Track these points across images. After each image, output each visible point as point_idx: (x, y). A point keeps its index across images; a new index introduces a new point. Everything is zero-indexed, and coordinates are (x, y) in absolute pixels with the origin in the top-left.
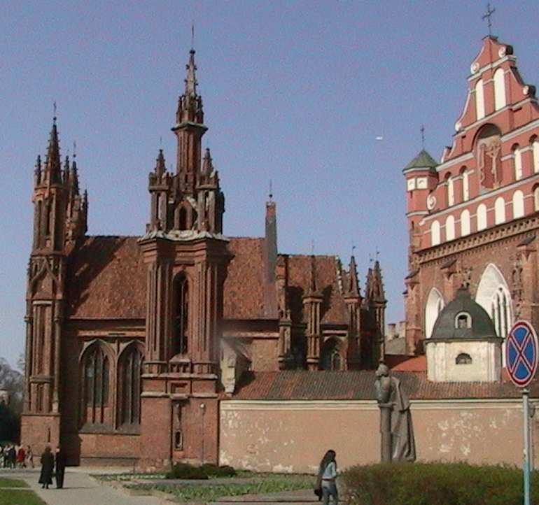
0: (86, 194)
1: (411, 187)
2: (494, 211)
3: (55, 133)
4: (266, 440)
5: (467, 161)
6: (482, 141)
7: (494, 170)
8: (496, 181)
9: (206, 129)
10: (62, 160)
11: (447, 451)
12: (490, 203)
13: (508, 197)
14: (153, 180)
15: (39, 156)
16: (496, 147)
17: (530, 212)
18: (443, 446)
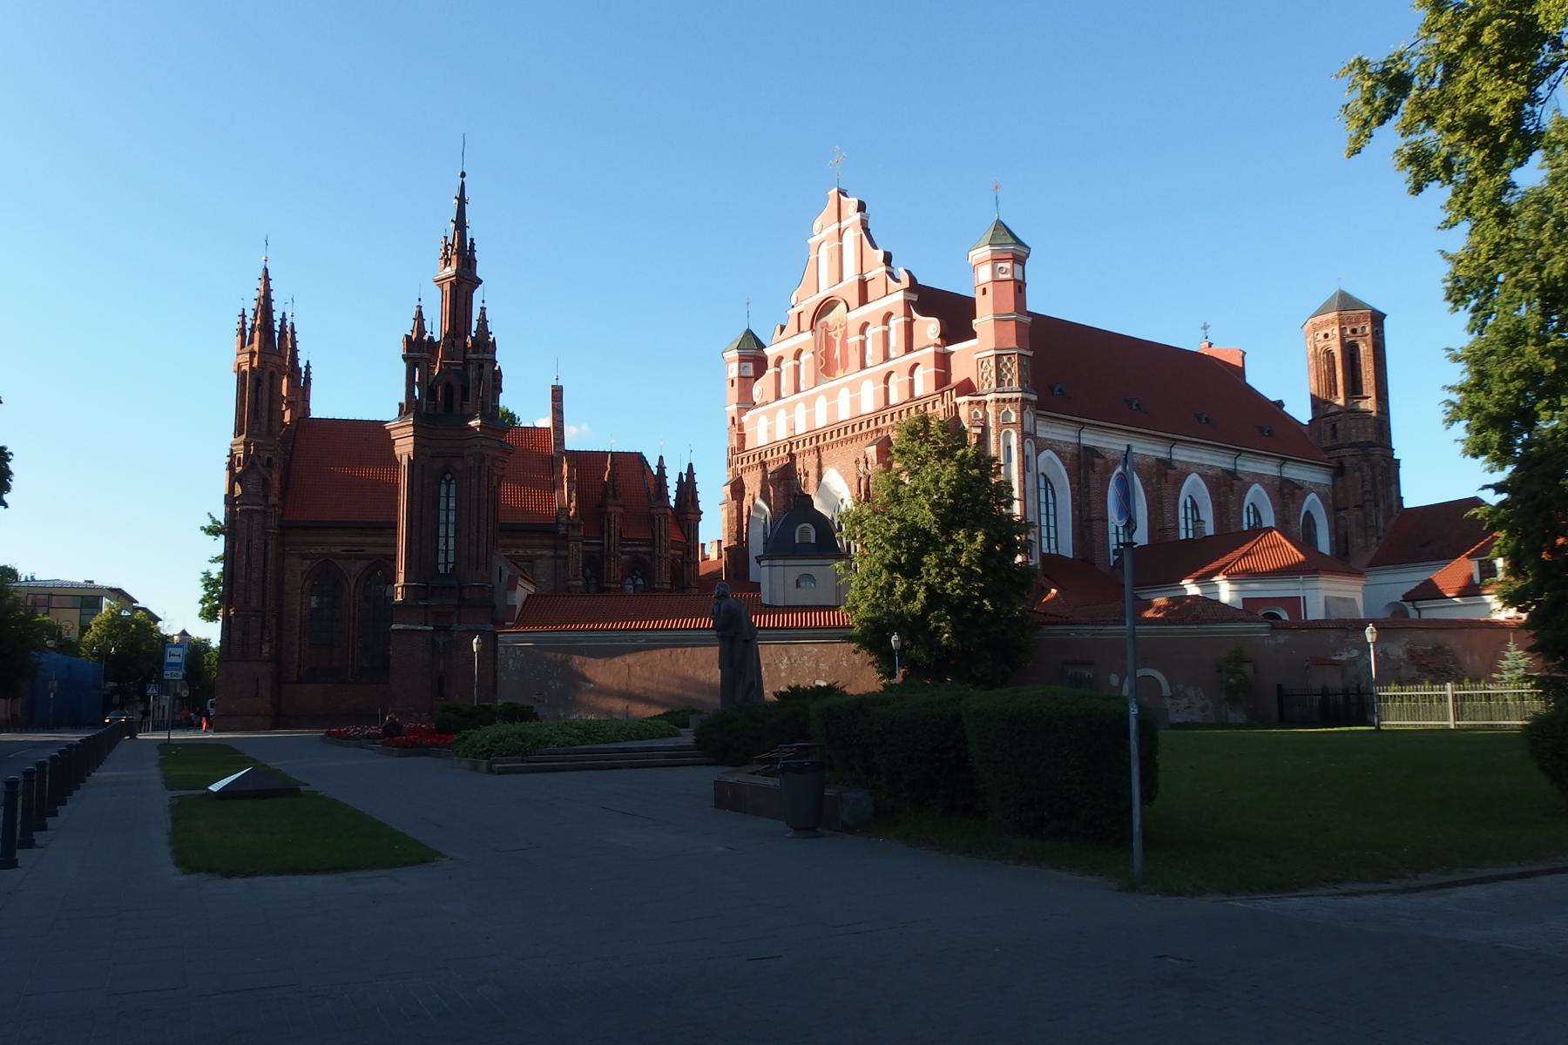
0: (308, 367)
2: (837, 404)
3: (267, 279)
4: (558, 684)
6: (824, 320)
8: (839, 366)
10: (277, 316)
12: (832, 395)
13: (854, 387)
16: (841, 327)
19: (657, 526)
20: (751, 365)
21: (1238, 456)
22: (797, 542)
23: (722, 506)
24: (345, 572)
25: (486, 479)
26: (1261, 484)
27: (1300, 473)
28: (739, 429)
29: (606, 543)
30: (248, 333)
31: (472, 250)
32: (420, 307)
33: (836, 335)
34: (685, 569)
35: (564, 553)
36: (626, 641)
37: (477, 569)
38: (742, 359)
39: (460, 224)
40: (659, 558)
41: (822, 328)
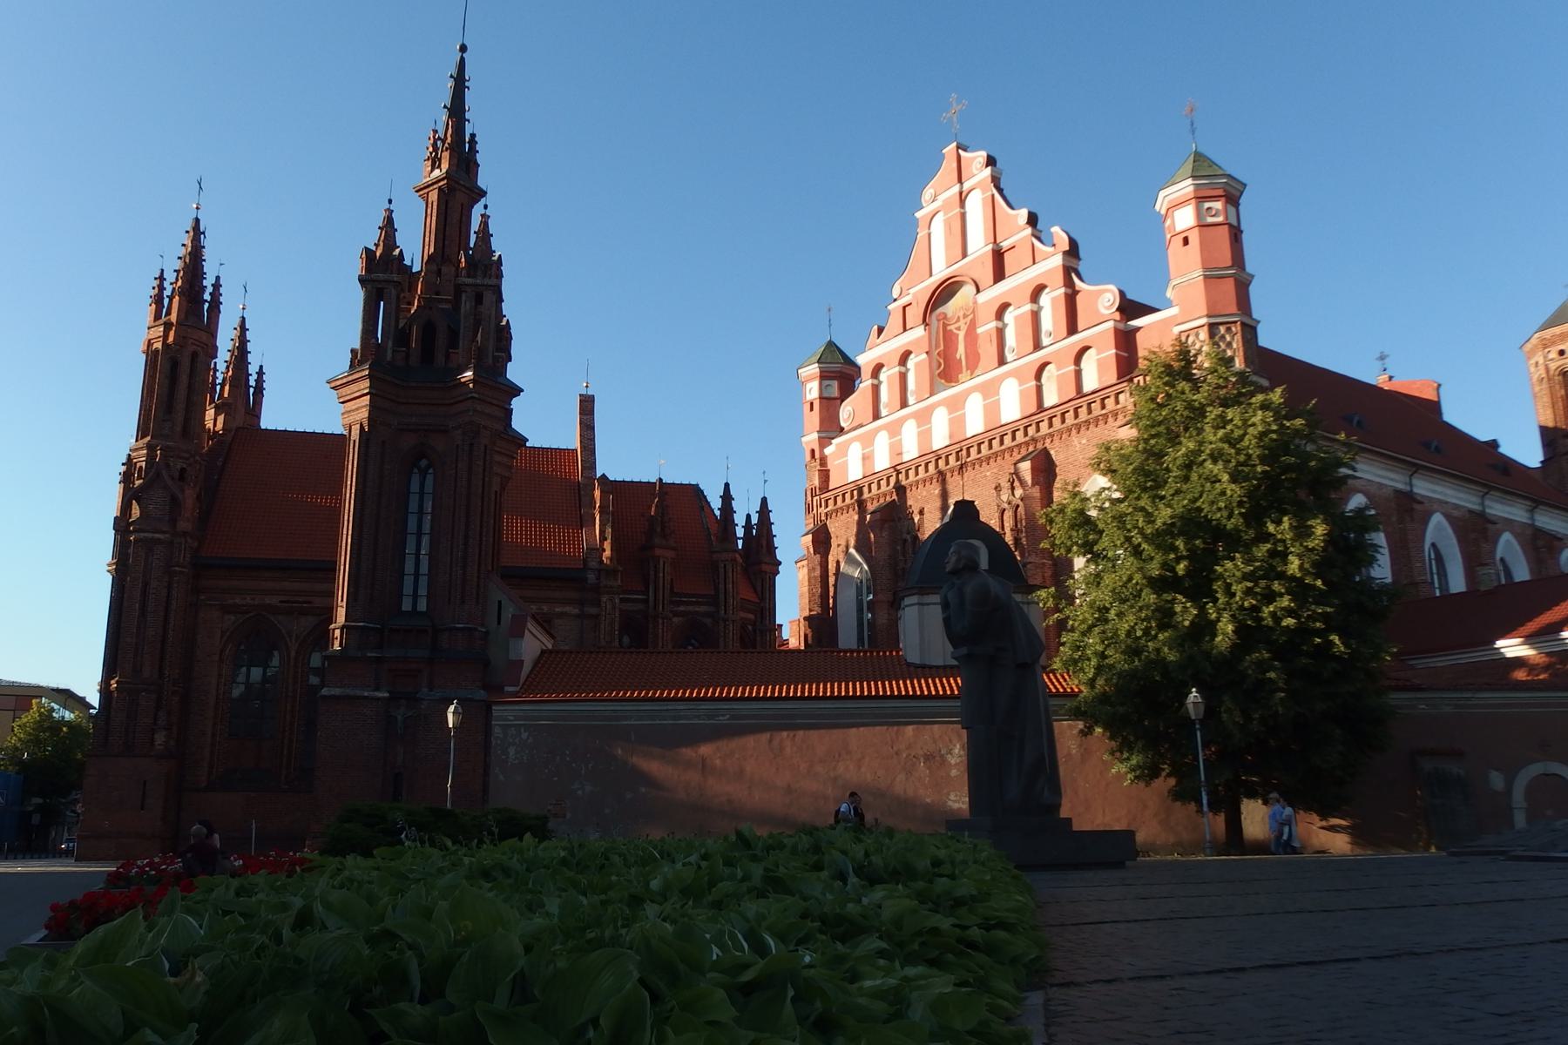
6: (940, 310)
7: (961, 351)
8: (964, 369)
9: (483, 194)
10: (208, 282)
12: (956, 405)
13: (990, 391)
18: (952, 797)
19: (722, 581)
20: (835, 384)
21: (1487, 493)
23: (799, 564)
24: (284, 631)
25: (481, 463)
26: (1512, 533)
27: (1553, 522)
28: (821, 465)
29: (651, 598)
30: (166, 301)
31: (473, 150)
32: (391, 212)
33: (958, 329)
34: (758, 639)
35: (593, 610)
36: (698, 717)
38: (824, 376)
39: (457, 110)
40: (725, 621)
41: (939, 320)
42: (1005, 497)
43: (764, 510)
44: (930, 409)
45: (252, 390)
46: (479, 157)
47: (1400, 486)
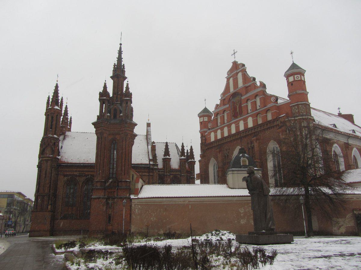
0: (71, 118)
1: (202, 120)
5: (225, 108)
9: (126, 78)
10: (60, 98)
11: (245, 223)
13: (245, 120)
14: (101, 95)
15: (49, 96)
17: (256, 124)
22: (242, 164)
31: (124, 68)
33: (237, 105)
35: (151, 174)
37: (124, 175)
39: (120, 59)
41: (232, 103)
42: (250, 146)
43: (191, 149)
44: (231, 124)
45: (69, 122)
46: (125, 70)
47: (346, 142)
